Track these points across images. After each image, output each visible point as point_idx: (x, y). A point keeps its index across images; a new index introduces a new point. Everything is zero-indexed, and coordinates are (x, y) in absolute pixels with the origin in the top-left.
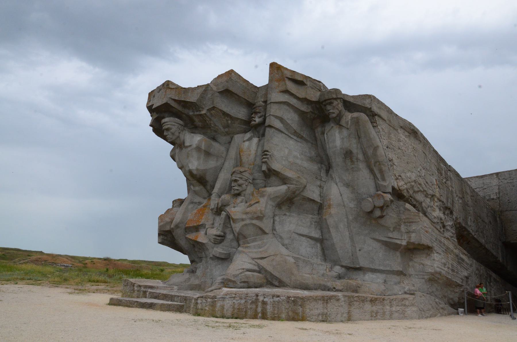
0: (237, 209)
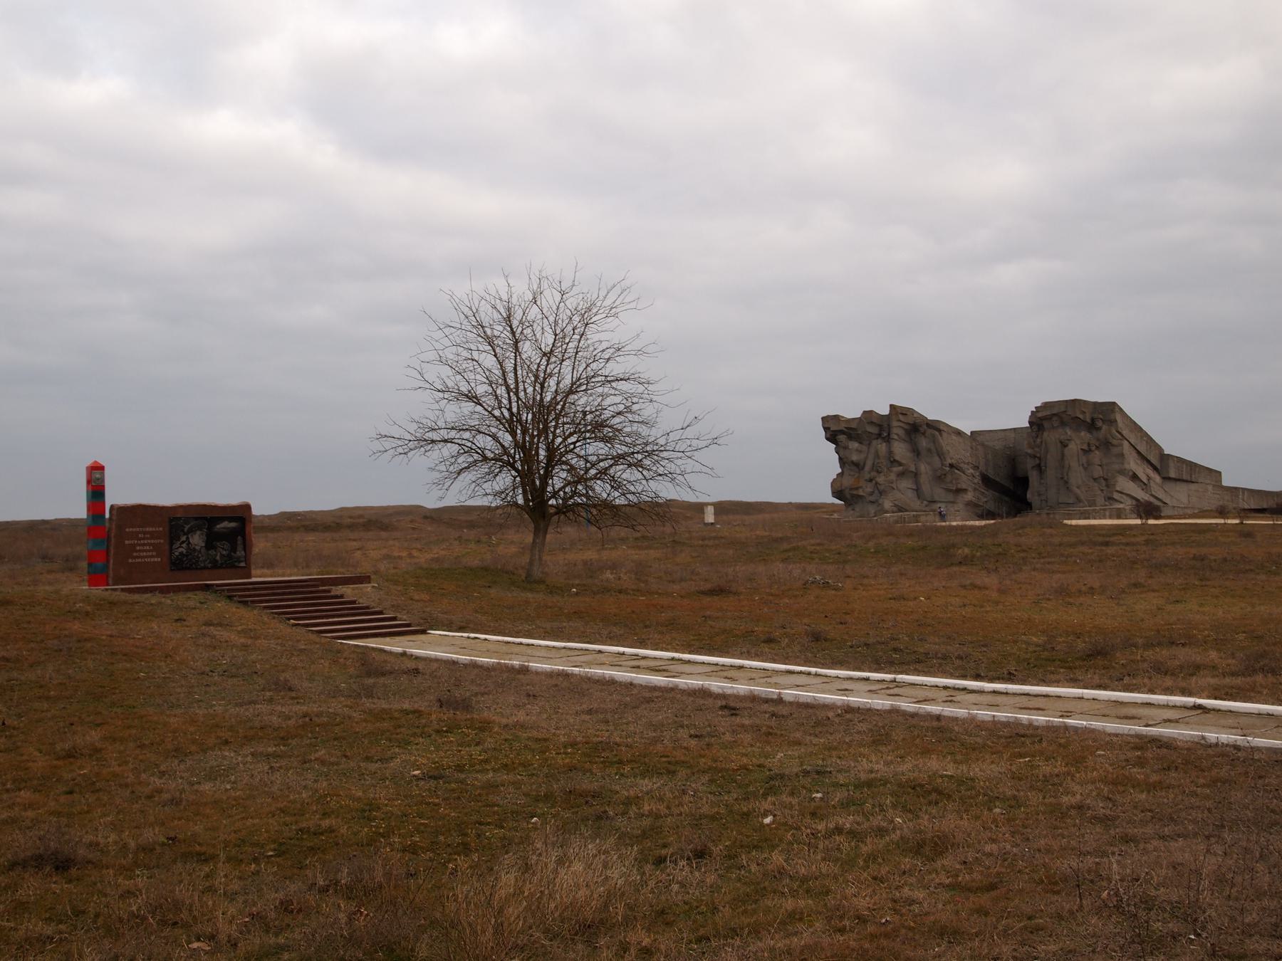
0: (881, 479)
